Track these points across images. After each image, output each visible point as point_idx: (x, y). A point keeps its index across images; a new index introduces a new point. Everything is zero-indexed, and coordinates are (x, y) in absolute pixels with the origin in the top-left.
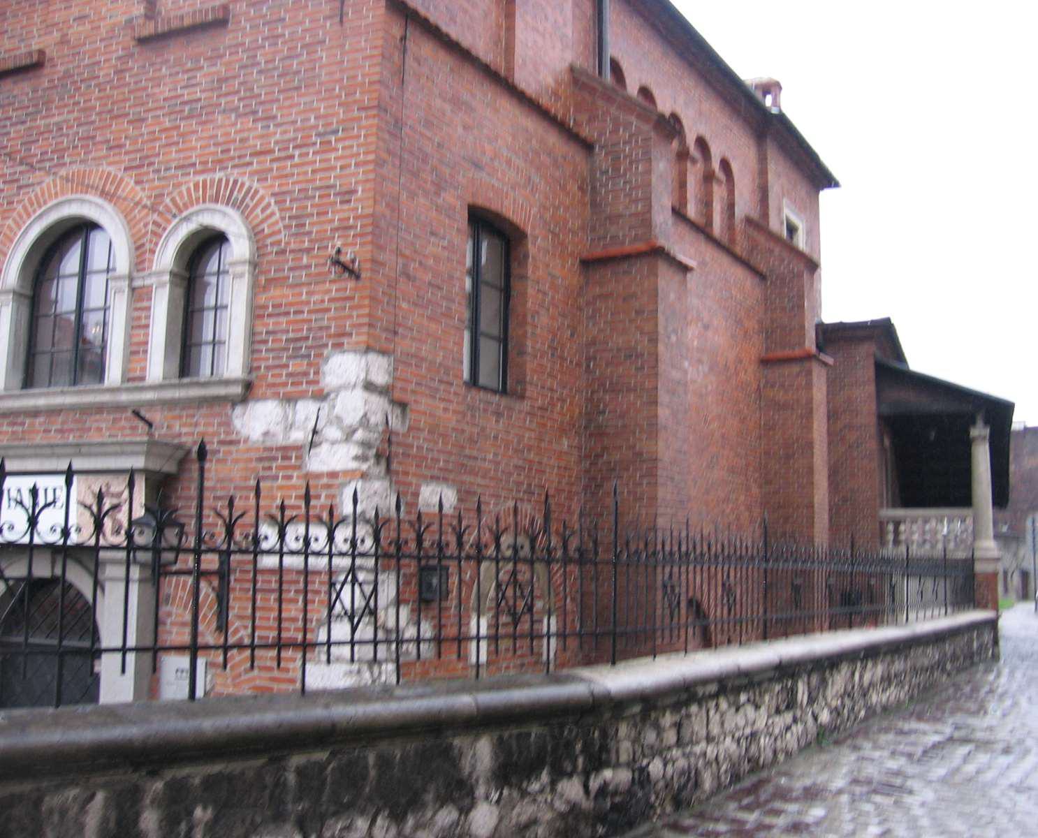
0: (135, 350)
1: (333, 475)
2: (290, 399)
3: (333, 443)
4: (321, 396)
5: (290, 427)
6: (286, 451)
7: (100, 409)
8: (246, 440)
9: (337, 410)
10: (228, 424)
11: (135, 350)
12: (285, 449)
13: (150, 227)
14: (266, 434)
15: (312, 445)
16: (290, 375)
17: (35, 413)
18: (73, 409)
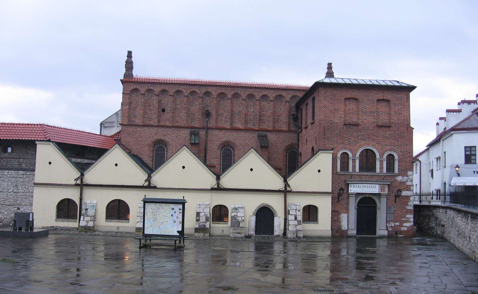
0: (381, 168)
1: (410, 185)
2: (403, 176)
3: (409, 182)
4: (407, 176)
5: (403, 179)
6: (403, 182)
7: (375, 175)
8: (398, 181)
9: (409, 178)
10: (395, 178)
11: (381, 168)
12: (403, 182)
13: (381, 152)
14: (400, 180)
15: (407, 182)
16: (403, 173)
17: (364, 175)
18: (371, 175)
